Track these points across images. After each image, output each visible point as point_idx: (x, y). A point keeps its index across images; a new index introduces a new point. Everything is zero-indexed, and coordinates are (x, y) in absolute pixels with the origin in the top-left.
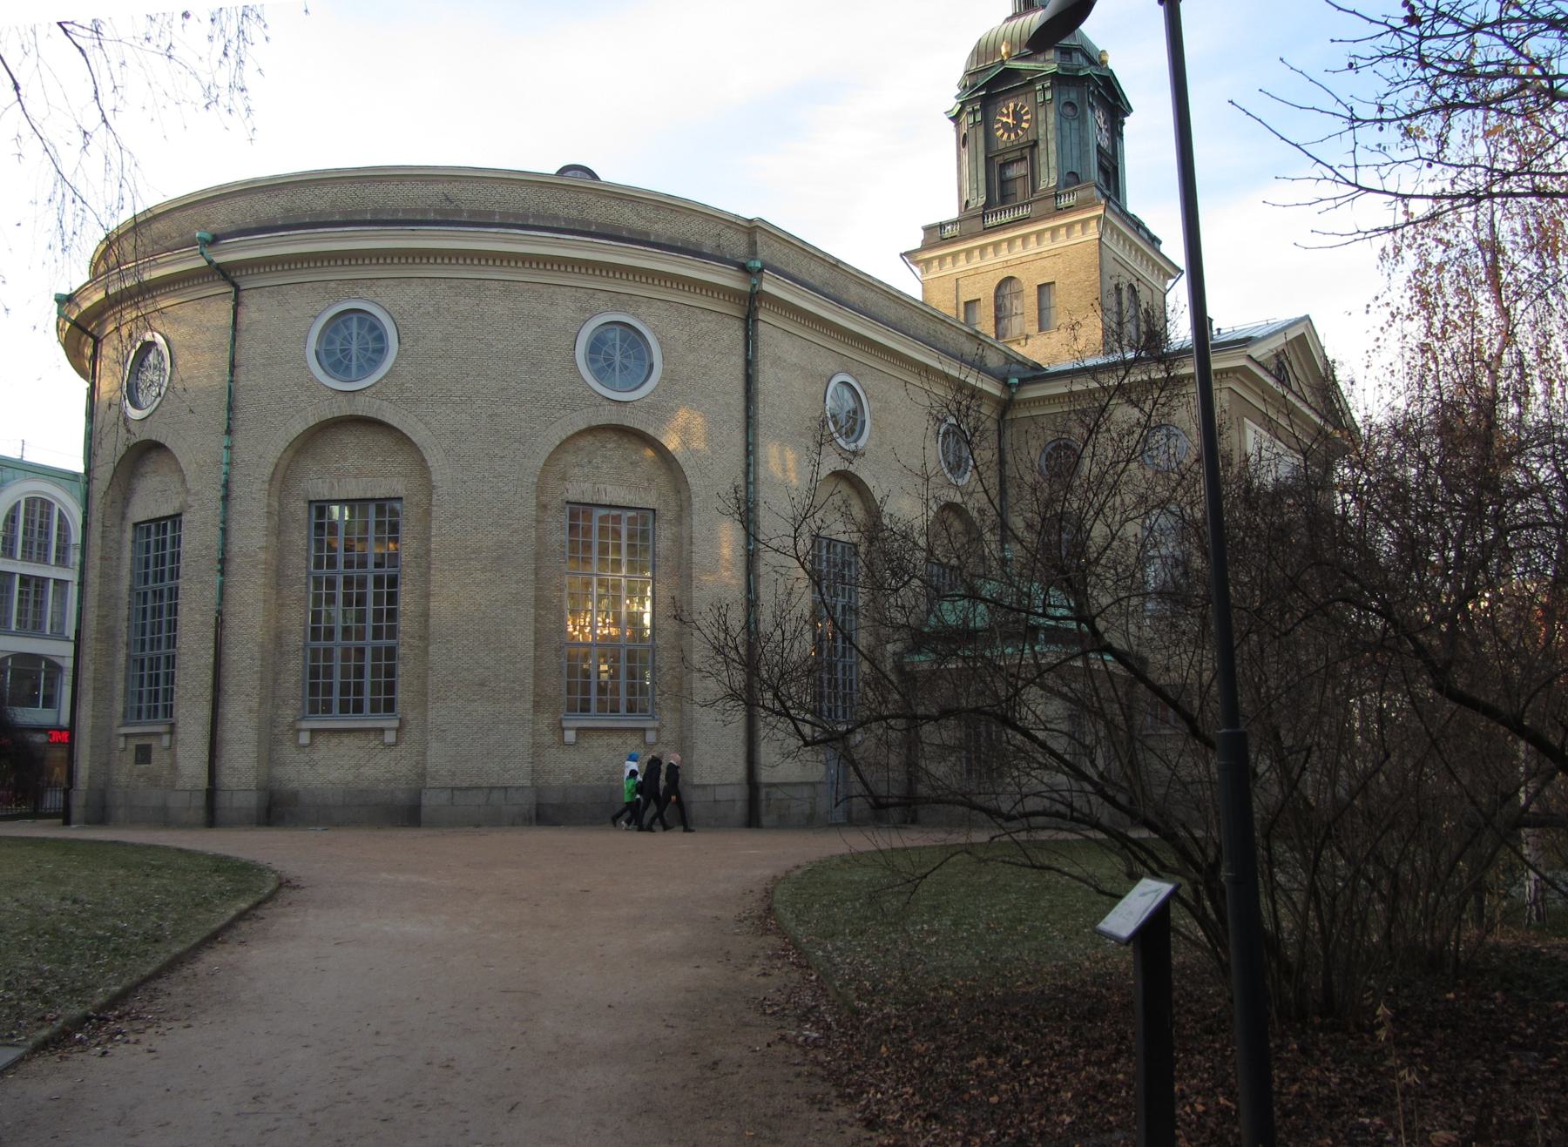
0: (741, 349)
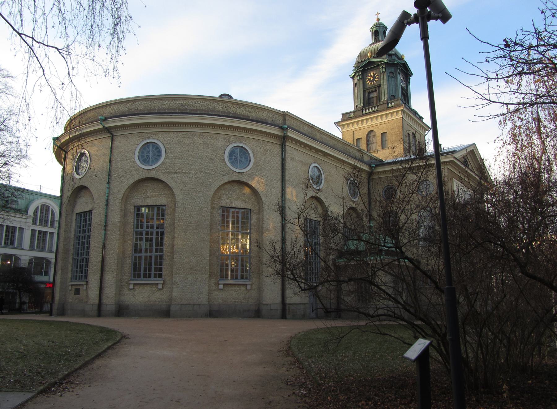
0: (280, 155)
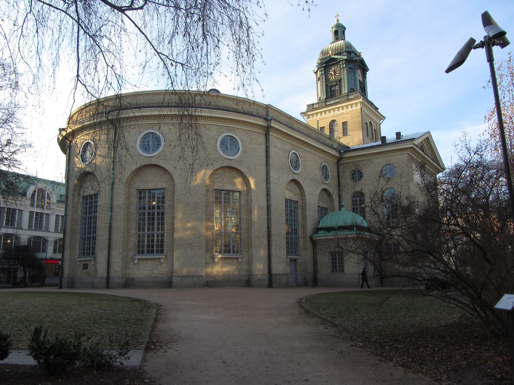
0: (264, 143)
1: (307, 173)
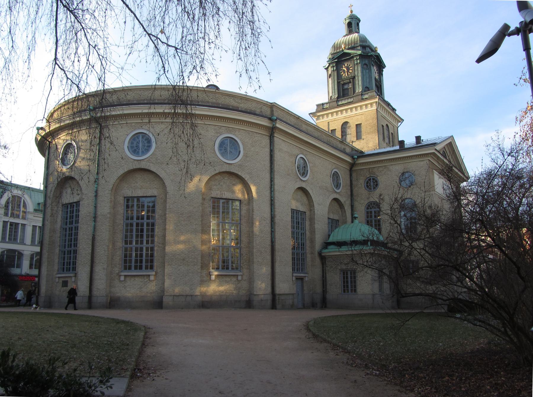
0: (268, 146)
1: (316, 180)
